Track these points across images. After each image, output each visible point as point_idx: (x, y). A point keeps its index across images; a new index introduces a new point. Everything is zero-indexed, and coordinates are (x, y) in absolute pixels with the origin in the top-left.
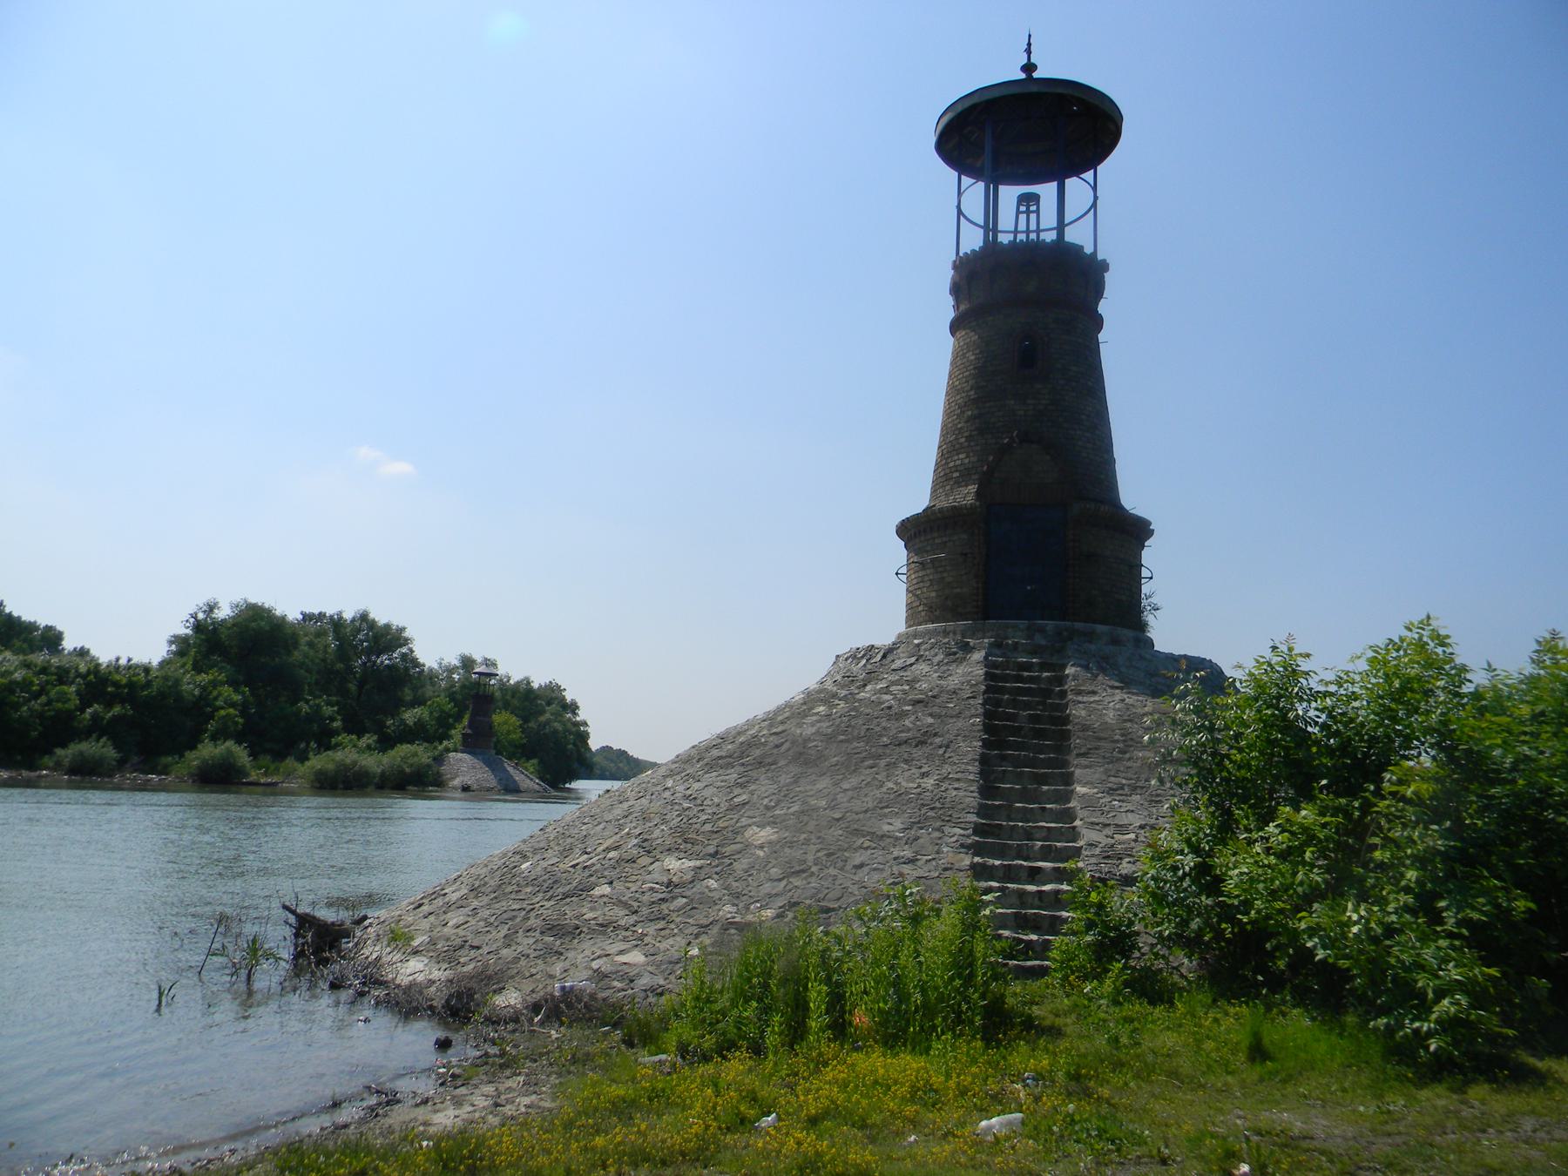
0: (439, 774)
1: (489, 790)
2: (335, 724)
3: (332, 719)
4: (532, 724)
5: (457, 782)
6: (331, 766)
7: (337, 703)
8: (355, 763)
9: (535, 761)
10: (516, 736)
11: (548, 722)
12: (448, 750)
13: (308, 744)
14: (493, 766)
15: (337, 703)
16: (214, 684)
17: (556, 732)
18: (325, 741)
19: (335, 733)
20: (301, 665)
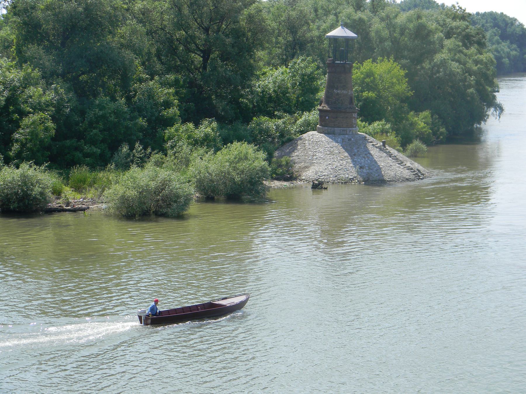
0: (289, 165)
1: (347, 182)
2: (171, 111)
3: (167, 105)
4: (426, 65)
5: (310, 174)
6: (132, 193)
7: (175, 84)
8: (165, 184)
9: (426, 113)
10: (402, 87)
11: (443, 63)
12: (308, 127)
13: (132, 148)
14: (355, 148)
15: (175, 84)
16: (27, 82)
17: (452, 74)
18: (154, 139)
19: (169, 122)
20: (129, 46)
